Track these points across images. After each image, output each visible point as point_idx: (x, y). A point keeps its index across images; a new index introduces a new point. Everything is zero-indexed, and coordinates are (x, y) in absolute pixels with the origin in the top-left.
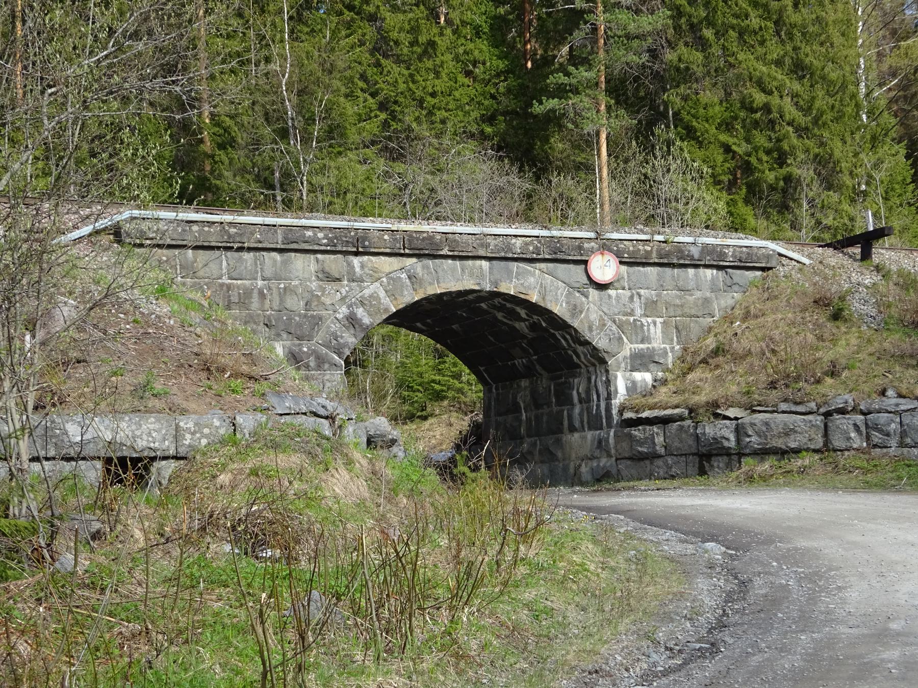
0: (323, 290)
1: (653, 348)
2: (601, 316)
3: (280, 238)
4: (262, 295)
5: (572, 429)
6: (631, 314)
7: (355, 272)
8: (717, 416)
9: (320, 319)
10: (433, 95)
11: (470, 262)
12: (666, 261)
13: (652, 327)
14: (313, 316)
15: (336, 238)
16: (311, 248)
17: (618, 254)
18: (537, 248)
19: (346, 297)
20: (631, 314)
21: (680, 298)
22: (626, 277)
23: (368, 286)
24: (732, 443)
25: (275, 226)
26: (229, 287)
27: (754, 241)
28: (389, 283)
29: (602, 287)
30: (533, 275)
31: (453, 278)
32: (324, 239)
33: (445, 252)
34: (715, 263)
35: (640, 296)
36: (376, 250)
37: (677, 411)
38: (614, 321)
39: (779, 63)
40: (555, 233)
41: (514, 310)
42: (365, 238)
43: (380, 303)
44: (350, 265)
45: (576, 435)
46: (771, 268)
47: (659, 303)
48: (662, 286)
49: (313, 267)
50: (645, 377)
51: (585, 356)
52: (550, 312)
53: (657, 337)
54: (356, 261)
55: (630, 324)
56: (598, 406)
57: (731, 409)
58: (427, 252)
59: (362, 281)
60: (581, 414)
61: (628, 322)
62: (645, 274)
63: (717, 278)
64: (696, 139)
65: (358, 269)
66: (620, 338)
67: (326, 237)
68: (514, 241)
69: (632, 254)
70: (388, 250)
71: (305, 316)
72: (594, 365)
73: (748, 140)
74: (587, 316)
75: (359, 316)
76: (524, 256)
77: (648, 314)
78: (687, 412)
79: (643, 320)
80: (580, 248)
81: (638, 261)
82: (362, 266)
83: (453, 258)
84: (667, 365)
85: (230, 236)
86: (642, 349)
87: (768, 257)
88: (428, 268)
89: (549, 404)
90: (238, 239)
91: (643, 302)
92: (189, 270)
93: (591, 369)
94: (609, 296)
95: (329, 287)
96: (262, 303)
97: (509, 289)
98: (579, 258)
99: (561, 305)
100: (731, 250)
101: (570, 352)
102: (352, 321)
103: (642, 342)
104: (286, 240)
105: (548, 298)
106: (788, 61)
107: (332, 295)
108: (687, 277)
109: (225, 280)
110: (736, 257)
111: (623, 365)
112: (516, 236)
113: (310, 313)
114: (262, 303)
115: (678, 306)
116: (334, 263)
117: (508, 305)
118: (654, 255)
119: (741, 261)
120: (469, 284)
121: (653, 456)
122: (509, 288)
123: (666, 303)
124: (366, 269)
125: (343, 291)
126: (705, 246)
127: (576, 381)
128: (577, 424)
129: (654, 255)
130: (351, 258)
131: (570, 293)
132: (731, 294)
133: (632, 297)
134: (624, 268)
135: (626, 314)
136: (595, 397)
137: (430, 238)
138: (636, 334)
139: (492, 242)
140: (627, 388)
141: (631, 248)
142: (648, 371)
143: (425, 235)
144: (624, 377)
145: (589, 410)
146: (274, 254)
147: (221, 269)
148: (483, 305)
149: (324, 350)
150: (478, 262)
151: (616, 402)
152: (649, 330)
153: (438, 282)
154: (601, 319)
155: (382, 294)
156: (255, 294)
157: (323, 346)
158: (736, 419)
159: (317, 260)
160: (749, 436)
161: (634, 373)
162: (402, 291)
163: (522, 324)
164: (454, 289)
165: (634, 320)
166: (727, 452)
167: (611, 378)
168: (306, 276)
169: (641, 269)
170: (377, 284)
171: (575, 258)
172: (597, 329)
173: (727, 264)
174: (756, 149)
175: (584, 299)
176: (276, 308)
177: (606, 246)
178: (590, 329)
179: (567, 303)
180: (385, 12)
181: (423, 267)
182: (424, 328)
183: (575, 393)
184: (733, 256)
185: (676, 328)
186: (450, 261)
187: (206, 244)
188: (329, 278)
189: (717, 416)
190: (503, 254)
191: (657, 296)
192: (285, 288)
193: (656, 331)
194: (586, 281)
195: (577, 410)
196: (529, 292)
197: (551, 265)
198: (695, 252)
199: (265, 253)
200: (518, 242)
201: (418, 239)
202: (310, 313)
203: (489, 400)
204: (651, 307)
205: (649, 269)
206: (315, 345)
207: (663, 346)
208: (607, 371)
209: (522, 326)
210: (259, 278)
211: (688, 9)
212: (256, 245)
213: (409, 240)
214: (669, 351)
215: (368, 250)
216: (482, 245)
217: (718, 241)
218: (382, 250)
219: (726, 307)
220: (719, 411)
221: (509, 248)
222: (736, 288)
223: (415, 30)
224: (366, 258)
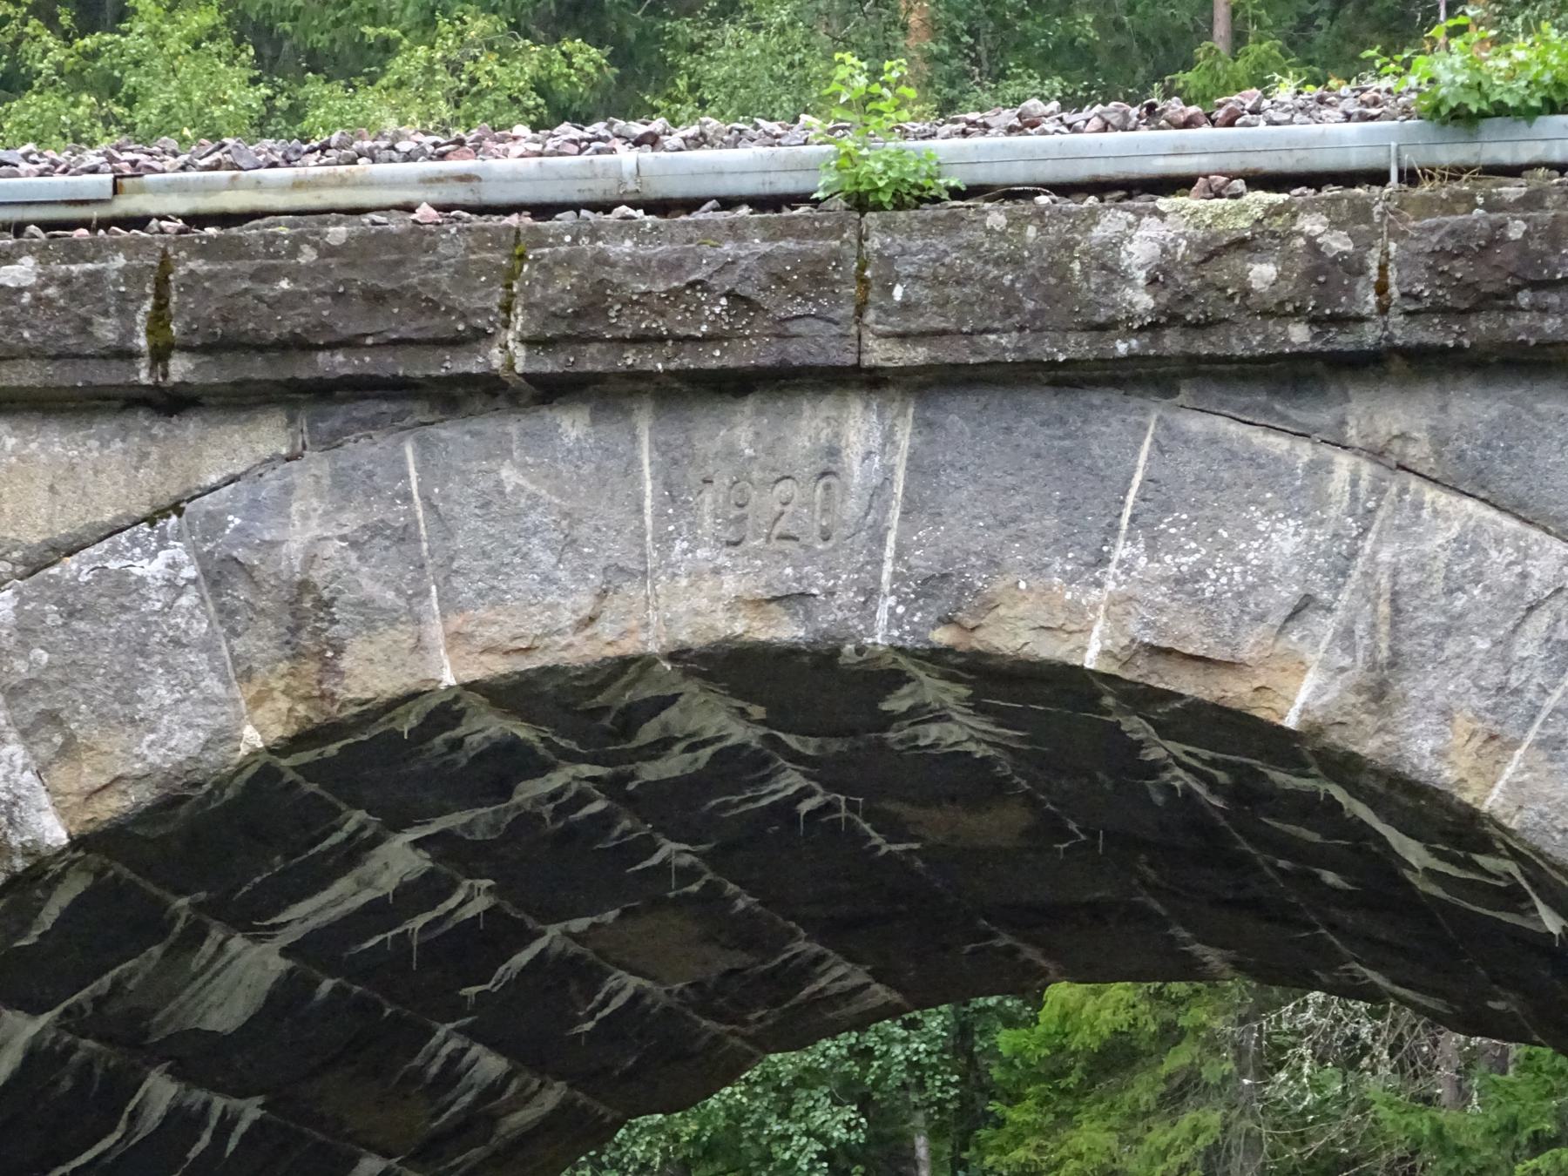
11: (741, 430)
30: (1304, 498)
33: (507, 353)
68: (1112, 221)
97: (1076, 621)
105: (1415, 687)
122: (1083, 614)
137: (381, 257)
150: (810, 425)
162: (126, 689)
164: (581, 651)
190: (1004, 344)
197: (1475, 409)
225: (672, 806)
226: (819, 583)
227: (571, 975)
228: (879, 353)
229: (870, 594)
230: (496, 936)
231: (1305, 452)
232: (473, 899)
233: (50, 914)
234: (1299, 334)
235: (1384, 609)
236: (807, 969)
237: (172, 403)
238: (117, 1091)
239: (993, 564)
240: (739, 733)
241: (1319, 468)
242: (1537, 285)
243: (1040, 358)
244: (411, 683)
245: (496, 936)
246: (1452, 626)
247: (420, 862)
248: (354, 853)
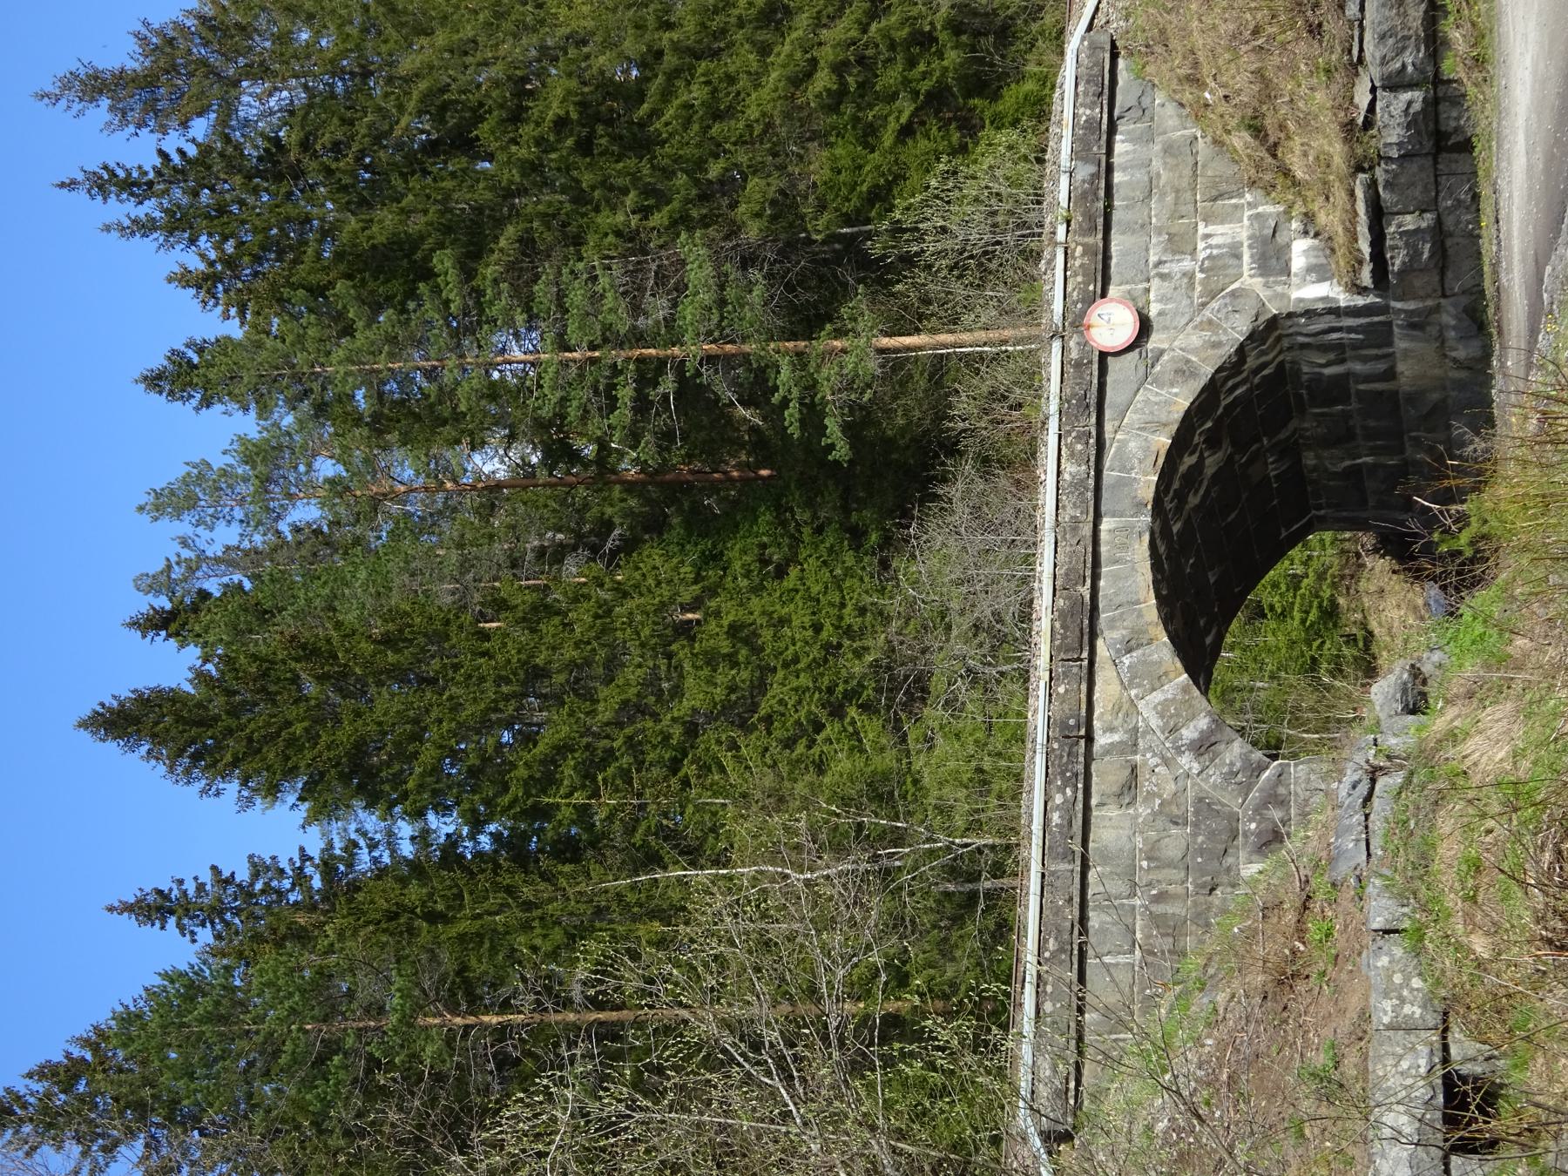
0: (1151, 795)
1: (1249, 238)
2: (1195, 327)
4: (1161, 898)
5: (1390, 374)
6: (1191, 276)
7: (1121, 742)
8: (1368, 124)
9: (1201, 800)
10: (817, 628)
11: (1103, 549)
12: (1100, 221)
13: (1213, 241)
14: (1197, 813)
15: (1063, 773)
16: (1080, 815)
17: (1089, 301)
18: (1078, 438)
19: (1163, 757)
20: (1190, 276)
21: (1163, 195)
22: (1128, 287)
23: (1144, 720)
24: (1417, 96)
25: (1043, 875)
27: (1067, 74)
28: (1139, 686)
29: (1145, 327)
30: (1124, 443)
31: (1131, 578)
32: (1064, 793)
33: (1085, 591)
34: (1104, 137)
35: (1160, 263)
36: (1084, 706)
37: (1359, 193)
38: (1204, 305)
39: (764, 50)
40: (1053, 407)
41: (1183, 476)
42: (1064, 725)
44: (1109, 750)
45: (1401, 367)
46: (1113, 43)
47: (1173, 231)
48: (1142, 226)
49: (1112, 812)
50: (1301, 251)
51: (1263, 353)
52: (1188, 412)
53: (1231, 231)
54: (1102, 740)
56: (1350, 330)
57: (1356, 100)
58: (1086, 622)
59: (1136, 729)
60: (1365, 360)
61: (1204, 282)
62: (1124, 254)
63: (1129, 133)
64: (890, 186)
65: (1116, 737)
66: (1233, 294)
67: (1062, 790)
68: (1067, 476)
69: (1089, 277)
70: (1084, 687)
71: (1196, 825)
72: (1279, 339)
73: (894, 97)
74: (1195, 351)
75: (1196, 735)
76: (1093, 459)
77: (1190, 248)
78: (1361, 176)
79: (1202, 255)
80: (1078, 365)
81: (1100, 267)
82: (1112, 729)
83: (1096, 577)
84: (1278, 214)
85: (1061, 950)
86: (1252, 256)
87: (1094, 48)
88: (1113, 620)
89: (1346, 416)
90: (1066, 936)
91: (1169, 257)
92: (1116, 1020)
93: (1285, 343)
94: (1160, 314)
95: (1146, 786)
96: (1175, 897)
98: (1095, 366)
99: (1176, 395)
100: (1081, 111)
101: (1257, 380)
102: (1204, 747)
103: (1239, 257)
104: (1068, 855)
105: (1163, 418)
106: (763, 36)
107: (1159, 781)
108: (1129, 183)
110: (1094, 103)
111: (1279, 289)
112: (1059, 473)
113: (1191, 818)
115: (1177, 198)
116: (1106, 777)
117: (1176, 485)
118: (1090, 240)
119: (1101, 94)
120: (1140, 551)
121: (1439, 233)
122: (1146, 483)
123: (1171, 218)
124: (1116, 723)
125: (1156, 760)
126: (1076, 155)
127: (1305, 369)
128: (1381, 366)
129: (1090, 240)
130: (1096, 748)
131: (1155, 381)
132: (1157, 109)
133: (1163, 277)
134: (1113, 291)
135: (1191, 286)
136: (1335, 336)
137: (1063, 617)
138: (1225, 267)
139: (1068, 513)
140: (1321, 280)
141: (1079, 279)
142: (1288, 246)
143: (1057, 625)
144: (1299, 287)
145: (1356, 346)
148: (1175, 528)
149: (1254, 794)
150: (1104, 536)
151: (1343, 299)
152: (1218, 246)
153: (1138, 602)
154: (1200, 327)
155: (1157, 697)
156: (1158, 909)
157: (1247, 795)
158: (1373, 90)
159: (1101, 805)
160: (1404, 66)
161: (1294, 269)
163: (1207, 462)
164: (1149, 577)
165: (1202, 271)
166: (1432, 104)
167: (1300, 308)
168: (1127, 824)
169: (1114, 262)
170: (1141, 705)
171: (1096, 373)
172: (1217, 334)
173: (1105, 116)
174: (906, 82)
175: (1166, 357)
176: (1183, 874)
177: (1076, 322)
178: (1216, 345)
179: (1172, 385)
180: (682, 708)
181: (1112, 628)
182: (1214, 631)
183: (1327, 371)
184: (1091, 107)
185: (1215, 199)
186: (1102, 583)
188: (1130, 786)
189: (1368, 124)
190: (1090, 495)
191: (1160, 234)
192: (1149, 859)
193: (1221, 234)
194: (1134, 354)
195: (1358, 367)
196: (1154, 449)
197: (1108, 414)
198: (1085, 171)
199: (1090, 892)
200: (1069, 468)
201: (1064, 637)
202: (1191, 818)
203: (1339, 520)
204: (1180, 244)
205: (1114, 249)
206: (1246, 810)
207: (1246, 222)
208: (1290, 315)
209: (1212, 463)
211: (676, 204)
213: (1067, 651)
214: (1254, 211)
215: (1083, 720)
216: (1075, 529)
217: (1067, 133)
218: (1083, 697)
219: (1180, 116)
220: (1360, 121)
221: (1078, 484)
222: (1146, 102)
223: (711, 659)
224: (1096, 724)
228: (1091, 517)
234: (1092, 441)
237: (1092, 663)
246: (1152, 413)
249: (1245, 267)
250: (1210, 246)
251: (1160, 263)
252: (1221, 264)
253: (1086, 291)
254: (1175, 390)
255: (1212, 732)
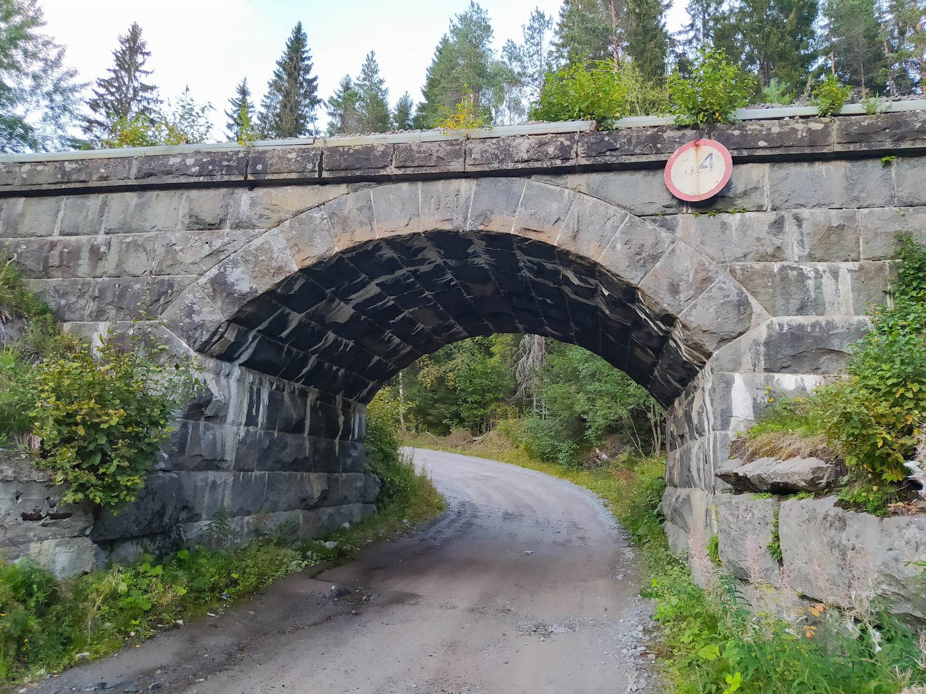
3: (134, 171)
11: (440, 185)
13: (827, 280)
14: (162, 282)
15: (210, 163)
16: (175, 181)
18: (562, 148)
19: (219, 251)
20: (777, 253)
26: (53, 245)
28: (291, 227)
32: (194, 165)
33: (392, 170)
35: (799, 221)
36: (275, 177)
38: (732, 272)
43: (271, 259)
54: (245, 196)
55: (772, 275)
59: (254, 227)
61: (766, 274)
66: (742, 305)
70: (294, 176)
75: (231, 279)
76: (537, 165)
79: (807, 268)
81: (793, 151)
82: (253, 204)
85: (64, 173)
86: (801, 327)
90: (74, 177)
94: (724, 225)
99: (614, 248)
102: (220, 285)
103: (801, 310)
105: (583, 236)
109: (56, 237)
114: (94, 266)
116: (208, 203)
118: (834, 137)
120: (429, 222)
125: (217, 244)
129: (834, 137)
131: (632, 225)
133: (778, 225)
135: (762, 258)
138: (787, 295)
140: (756, 406)
142: (815, 370)
144: (746, 383)
146: (128, 195)
147: (55, 223)
150: (455, 184)
152: (818, 287)
159: (190, 201)
161: (777, 376)
162: (311, 238)
165: (783, 269)
169: (804, 169)
171: (644, 159)
176: (111, 272)
178: (674, 289)
187: (35, 188)
188: (199, 224)
190: (495, 166)
196: (547, 227)
197: (595, 178)
201: (342, 154)
207: (856, 319)
210: (102, 231)
212: (99, 184)
215: (261, 177)
216: (456, 154)
224: (260, 192)
225: (426, 279)
226: (454, 216)
227: (410, 323)
228: (469, 169)
229: (466, 219)
230: (393, 311)
231: (558, 189)
232: (390, 301)
233: (296, 287)
234: (558, 163)
235: (576, 220)
236: (451, 326)
237: (323, 182)
238: (321, 335)
239: (492, 212)
240: (440, 261)
241: (561, 192)
242: (610, 150)
243: (503, 171)
244: (370, 238)
245: (393, 311)
247: (377, 290)
248: (364, 285)
249: (785, 319)
250: (818, 275)
251: (799, 221)
252: (792, 289)
253: (757, 138)
254: (619, 246)
255: (230, 294)
